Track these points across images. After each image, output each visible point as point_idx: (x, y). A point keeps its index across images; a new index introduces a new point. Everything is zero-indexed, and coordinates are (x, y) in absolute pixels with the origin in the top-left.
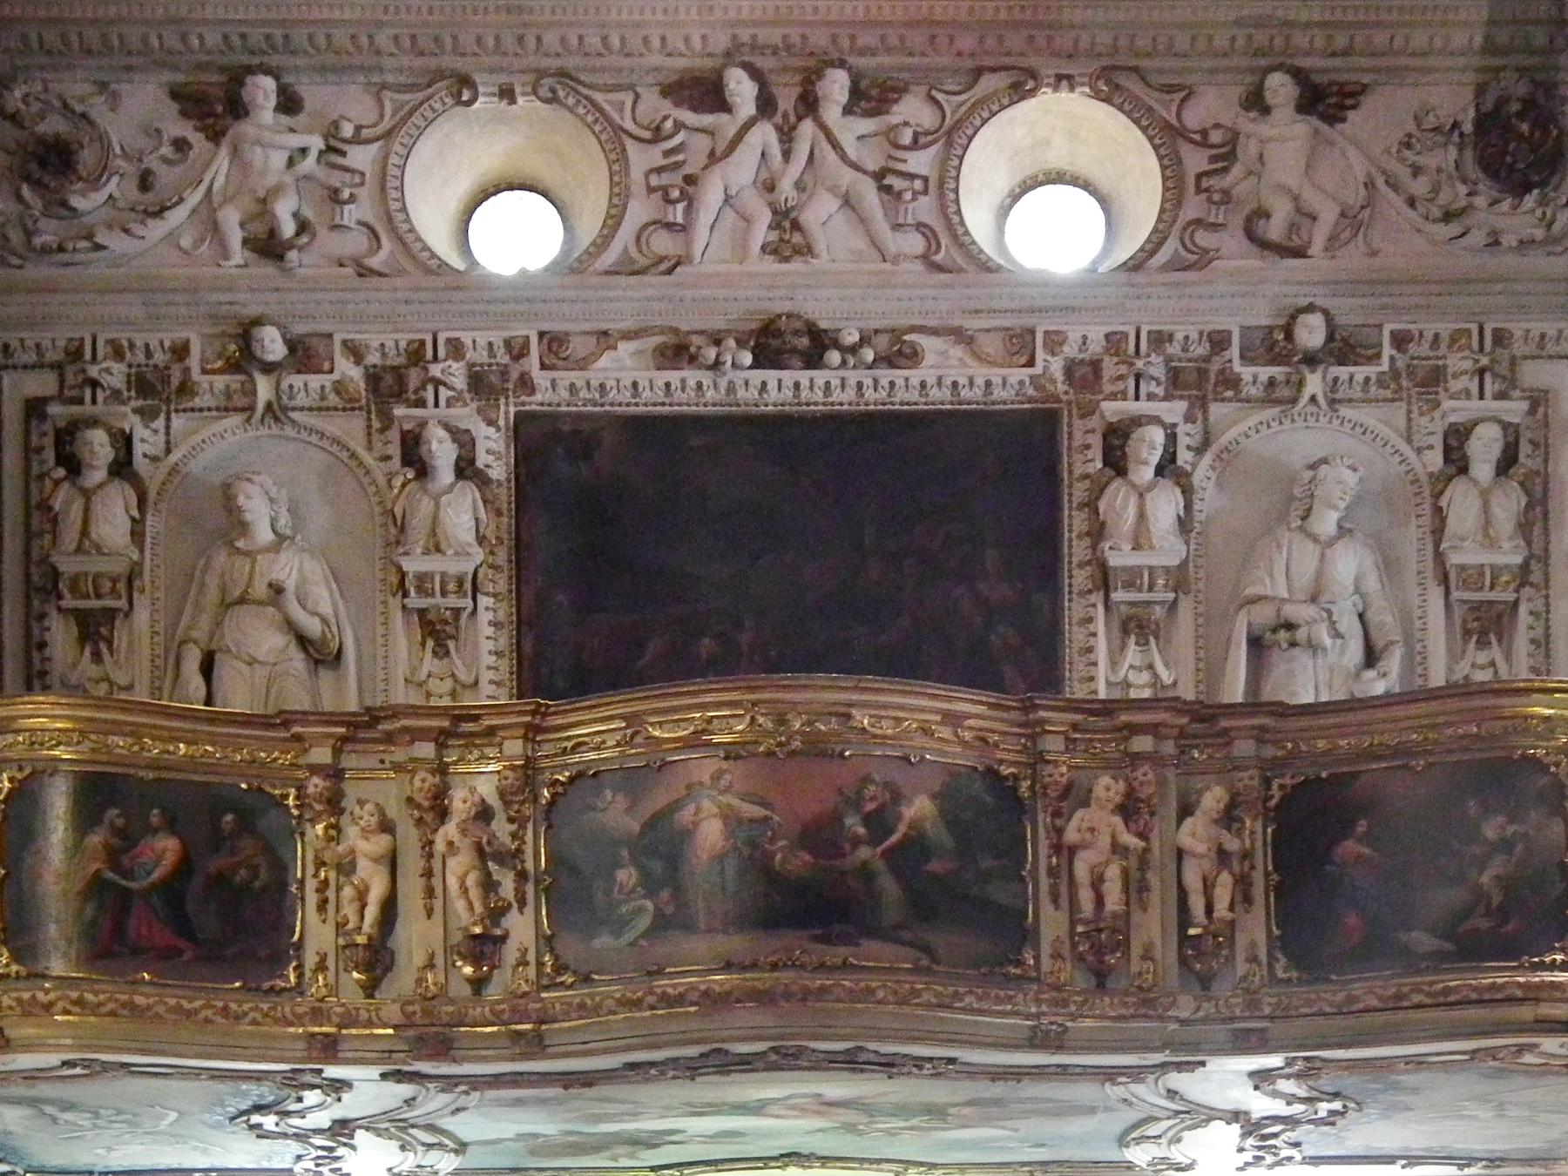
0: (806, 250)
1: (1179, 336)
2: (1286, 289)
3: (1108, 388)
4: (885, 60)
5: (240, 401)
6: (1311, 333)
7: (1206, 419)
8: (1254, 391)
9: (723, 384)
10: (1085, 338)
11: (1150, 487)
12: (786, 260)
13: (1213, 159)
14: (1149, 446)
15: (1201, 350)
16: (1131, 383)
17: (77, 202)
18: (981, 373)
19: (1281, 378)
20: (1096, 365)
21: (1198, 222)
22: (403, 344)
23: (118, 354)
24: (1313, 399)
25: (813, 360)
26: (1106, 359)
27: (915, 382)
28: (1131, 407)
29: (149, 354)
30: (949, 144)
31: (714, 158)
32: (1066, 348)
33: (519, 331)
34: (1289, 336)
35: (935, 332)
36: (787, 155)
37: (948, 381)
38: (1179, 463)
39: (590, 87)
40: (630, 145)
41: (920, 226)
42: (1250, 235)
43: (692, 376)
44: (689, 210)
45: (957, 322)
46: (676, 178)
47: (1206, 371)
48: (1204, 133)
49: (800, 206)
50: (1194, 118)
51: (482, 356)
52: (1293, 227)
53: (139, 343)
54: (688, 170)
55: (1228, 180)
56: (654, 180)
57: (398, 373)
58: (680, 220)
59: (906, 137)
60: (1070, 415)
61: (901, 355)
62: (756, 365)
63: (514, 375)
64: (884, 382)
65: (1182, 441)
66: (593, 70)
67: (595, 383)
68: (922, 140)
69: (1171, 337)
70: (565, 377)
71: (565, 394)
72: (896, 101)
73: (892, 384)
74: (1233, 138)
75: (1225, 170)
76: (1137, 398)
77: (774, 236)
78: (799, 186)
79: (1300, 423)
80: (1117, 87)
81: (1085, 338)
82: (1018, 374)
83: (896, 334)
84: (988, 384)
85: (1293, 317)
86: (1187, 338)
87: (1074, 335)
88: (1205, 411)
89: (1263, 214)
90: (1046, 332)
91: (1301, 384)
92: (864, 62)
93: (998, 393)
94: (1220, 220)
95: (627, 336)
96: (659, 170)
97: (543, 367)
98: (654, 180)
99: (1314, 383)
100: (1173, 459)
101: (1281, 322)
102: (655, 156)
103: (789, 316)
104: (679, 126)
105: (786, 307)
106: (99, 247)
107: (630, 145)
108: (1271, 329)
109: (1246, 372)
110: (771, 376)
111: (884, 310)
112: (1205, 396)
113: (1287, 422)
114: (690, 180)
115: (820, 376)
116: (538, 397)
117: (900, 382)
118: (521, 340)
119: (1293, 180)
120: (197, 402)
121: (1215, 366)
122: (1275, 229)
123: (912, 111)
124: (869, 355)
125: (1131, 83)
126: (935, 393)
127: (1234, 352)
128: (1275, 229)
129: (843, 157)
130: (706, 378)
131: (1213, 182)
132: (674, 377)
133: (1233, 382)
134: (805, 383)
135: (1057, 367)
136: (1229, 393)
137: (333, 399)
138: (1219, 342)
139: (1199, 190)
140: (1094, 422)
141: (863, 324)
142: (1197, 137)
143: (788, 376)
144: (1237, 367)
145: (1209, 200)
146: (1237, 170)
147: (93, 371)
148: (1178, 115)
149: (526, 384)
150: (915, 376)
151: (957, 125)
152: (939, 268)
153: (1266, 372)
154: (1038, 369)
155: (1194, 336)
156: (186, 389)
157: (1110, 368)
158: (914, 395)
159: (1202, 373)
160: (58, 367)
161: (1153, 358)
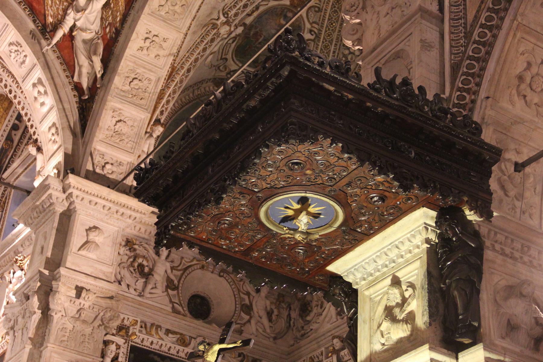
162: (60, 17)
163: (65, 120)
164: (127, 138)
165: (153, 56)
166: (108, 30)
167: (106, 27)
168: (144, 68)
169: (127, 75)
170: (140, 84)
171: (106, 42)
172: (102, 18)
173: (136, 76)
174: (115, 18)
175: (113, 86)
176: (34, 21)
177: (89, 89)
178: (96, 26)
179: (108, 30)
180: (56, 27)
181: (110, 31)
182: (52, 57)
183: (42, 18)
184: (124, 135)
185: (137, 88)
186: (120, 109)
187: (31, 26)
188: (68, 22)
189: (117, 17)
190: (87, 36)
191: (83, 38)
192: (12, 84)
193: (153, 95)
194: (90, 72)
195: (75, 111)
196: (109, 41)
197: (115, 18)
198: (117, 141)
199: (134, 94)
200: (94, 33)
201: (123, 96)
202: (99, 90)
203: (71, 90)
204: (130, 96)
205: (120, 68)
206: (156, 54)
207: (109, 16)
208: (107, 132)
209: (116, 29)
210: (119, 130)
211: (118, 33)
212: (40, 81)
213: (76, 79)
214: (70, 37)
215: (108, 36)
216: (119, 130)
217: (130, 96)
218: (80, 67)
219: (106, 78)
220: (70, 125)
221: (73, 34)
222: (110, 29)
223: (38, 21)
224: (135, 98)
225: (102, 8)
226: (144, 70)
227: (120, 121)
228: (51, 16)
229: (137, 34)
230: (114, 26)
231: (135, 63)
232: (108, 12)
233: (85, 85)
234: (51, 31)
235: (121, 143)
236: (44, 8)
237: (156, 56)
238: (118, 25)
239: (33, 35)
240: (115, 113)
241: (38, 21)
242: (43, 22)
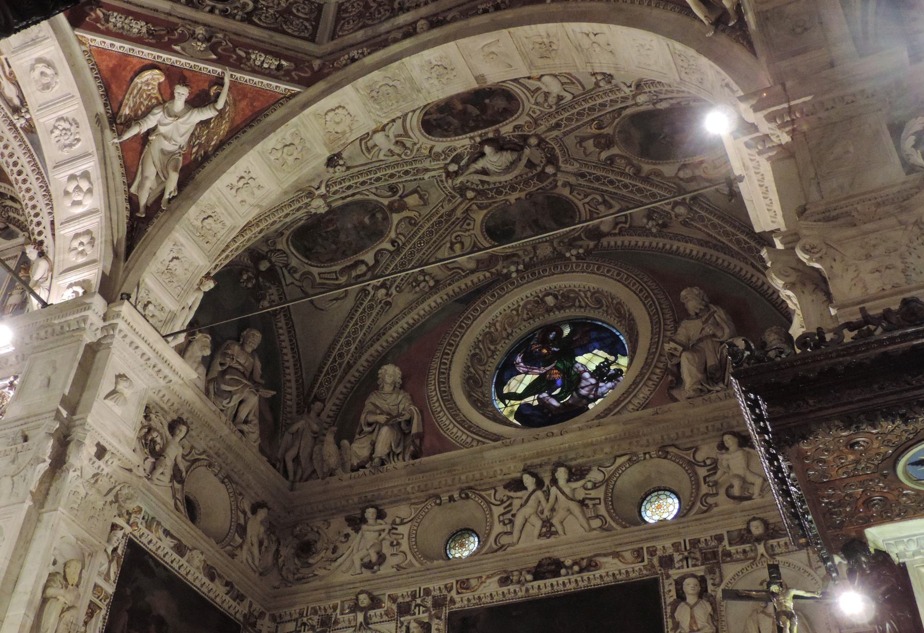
0: (556, 533)
1: (702, 540)
2: (744, 513)
3: (677, 565)
4: (580, 461)
5: (353, 624)
6: (757, 529)
7: (720, 571)
8: (738, 556)
9: (524, 589)
10: (664, 547)
11: (696, 604)
12: (549, 538)
13: (708, 471)
14: (690, 586)
15: (714, 543)
16: (685, 563)
17: (311, 561)
18: (623, 567)
19: (748, 549)
20: (670, 558)
21: (707, 495)
22: (409, 593)
23: (315, 612)
24: (762, 555)
25: (556, 574)
26: (675, 554)
27: (597, 576)
28: (685, 570)
29: (325, 610)
30: (607, 485)
31: (522, 506)
32: (658, 553)
33: (448, 581)
34: (748, 531)
35: (605, 555)
36: (548, 500)
37: (610, 573)
38: (709, 591)
39: (479, 491)
40: (493, 507)
41: (597, 516)
42: (729, 495)
43: (512, 588)
44: (513, 526)
45: (613, 549)
46: (509, 516)
47: (718, 551)
48: (704, 462)
49: (552, 517)
50: (700, 457)
51: (437, 593)
52: (743, 488)
53: (322, 607)
54: (513, 512)
55: (716, 477)
56: (501, 518)
57: (408, 604)
58: (509, 530)
59: (589, 485)
60: (663, 579)
61: (591, 565)
62: (535, 579)
63: (449, 598)
64: (585, 578)
65: (709, 582)
66: (480, 485)
67: (476, 597)
68: (597, 485)
69: (699, 541)
70: (468, 595)
71: (466, 603)
72: (587, 474)
73: (589, 578)
74: (715, 462)
75: (715, 473)
76: (688, 567)
77: (544, 530)
78: (553, 510)
79: (760, 565)
80: (668, 452)
81: (664, 547)
82: (638, 566)
83: (590, 560)
84: (627, 572)
85: (748, 523)
86: (706, 540)
87: (659, 547)
88: (720, 568)
89: (732, 486)
90: (648, 548)
91: (756, 550)
92: (573, 463)
93: (632, 575)
94: (715, 492)
95: (488, 577)
96: (503, 514)
97: (458, 593)
98: (501, 518)
99: (761, 549)
100: (706, 591)
101: (745, 526)
102: (501, 509)
103: (546, 559)
104: (509, 498)
105: (547, 555)
106: (315, 575)
107: (493, 507)
108: (740, 530)
109: (733, 549)
110: (541, 583)
111: (585, 551)
112: (718, 562)
113: (754, 567)
114: (514, 515)
115: (560, 580)
116: (457, 605)
117: (592, 577)
118: (450, 585)
119: (741, 472)
120: (339, 626)
121: (720, 550)
122: (736, 491)
123: (595, 475)
124: (576, 568)
125: (672, 450)
126: (607, 579)
127: (726, 542)
128: (736, 491)
129: (567, 496)
130: (517, 587)
131: (711, 479)
132: (505, 589)
133: (728, 554)
134: (555, 583)
135: (655, 561)
136: (729, 559)
137: (385, 618)
138: (719, 538)
139: (705, 482)
140: (671, 581)
141: (575, 558)
142: (702, 464)
143: (548, 582)
144: (728, 548)
145: (709, 486)
146: (719, 473)
147: (305, 620)
148: (694, 457)
149: (453, 601)
150: (597, 573)
151: (610, 478)
152: (606, 530)
153: (740, 548)
154: (646, 562)
155: (708, 538)
156: (336, 622)
157: (677, 557)
158: (598, 581)
159: (715, 554)
160: (296, 620)
161: (693, 550)
162: (140, 112)
163: (110, 232)
164: (177, 281)
165: (239, 199)
166: (194, 150)
167: (194, 147)
168: (226, 210)
169: (204, 209)
170: (214, 225)
171: (187, 162)
172: (193, 134)
173: (213, 215)
174: (209, 140)
175: (186, 215)
176: (105, 105)
177: (147, 207)
178: (183, 141)
179: (194, 150)
180: (128, 123)
181: (197, 152)
182: (113, 154)
183: (115, 105)
184: (176, 276)
185: (208, 227)
186: (182, 245)
187: (101, 109)
188: (149, 123)
189: (212, 140)
190: (169, 147)
191: (162, 147)
192: (26, 165)
193: (221, 243)
194: (154, 188)
195: (123, 226)
196: (191, 162)
197: (209, 140)
198: (167, 281)
199: (202, 234)
200: (177, 147)
201: (191, 231)
202: (161, 214)
203: (124, 201)
204: (198, 234)
205: (201, 198)
206: (243, 199)
207: (203, 136)
208: (160, 266)
209: (206, 153)
210: (174, 269)
211: (206, 158)
212: (86, 175)
213: (133, 189)
214: (144, 139)
215: (193, 157)
216: (174, 269)
217: (198, 234)
218: (144, 178)
219: (174, 204)
220: (113, 241)
221: (150, 138)
222: (198, 150)
223: (109, 107)
224: (201, 239)
225: (198, 124)
226: (224, 212)
227: (177, 258)
228: (129, 108)
229: (236, 168)
230: (204, 149)
231: (219, 198)
232: (203, 131)
233: (143, 200)
234: (121, 124)
235: (170, 284)
236: (124, 96)
237: (242, 201)
238: (210, 149)
239: (98, 119)
240: (176, 247)
241: (109, 107)
242: (116, 110)
